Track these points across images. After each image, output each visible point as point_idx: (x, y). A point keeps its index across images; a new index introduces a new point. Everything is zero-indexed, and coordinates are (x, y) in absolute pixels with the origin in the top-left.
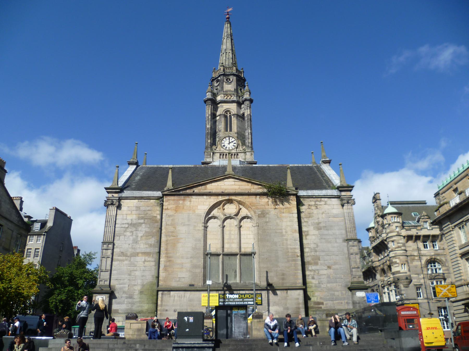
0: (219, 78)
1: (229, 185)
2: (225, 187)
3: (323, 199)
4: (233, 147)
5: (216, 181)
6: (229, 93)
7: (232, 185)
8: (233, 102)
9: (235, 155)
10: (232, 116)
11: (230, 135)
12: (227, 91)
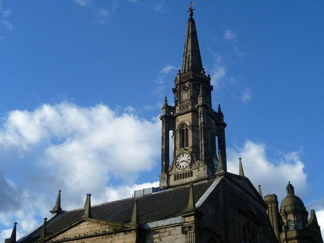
3: (167, 229)
5: (74, 226)
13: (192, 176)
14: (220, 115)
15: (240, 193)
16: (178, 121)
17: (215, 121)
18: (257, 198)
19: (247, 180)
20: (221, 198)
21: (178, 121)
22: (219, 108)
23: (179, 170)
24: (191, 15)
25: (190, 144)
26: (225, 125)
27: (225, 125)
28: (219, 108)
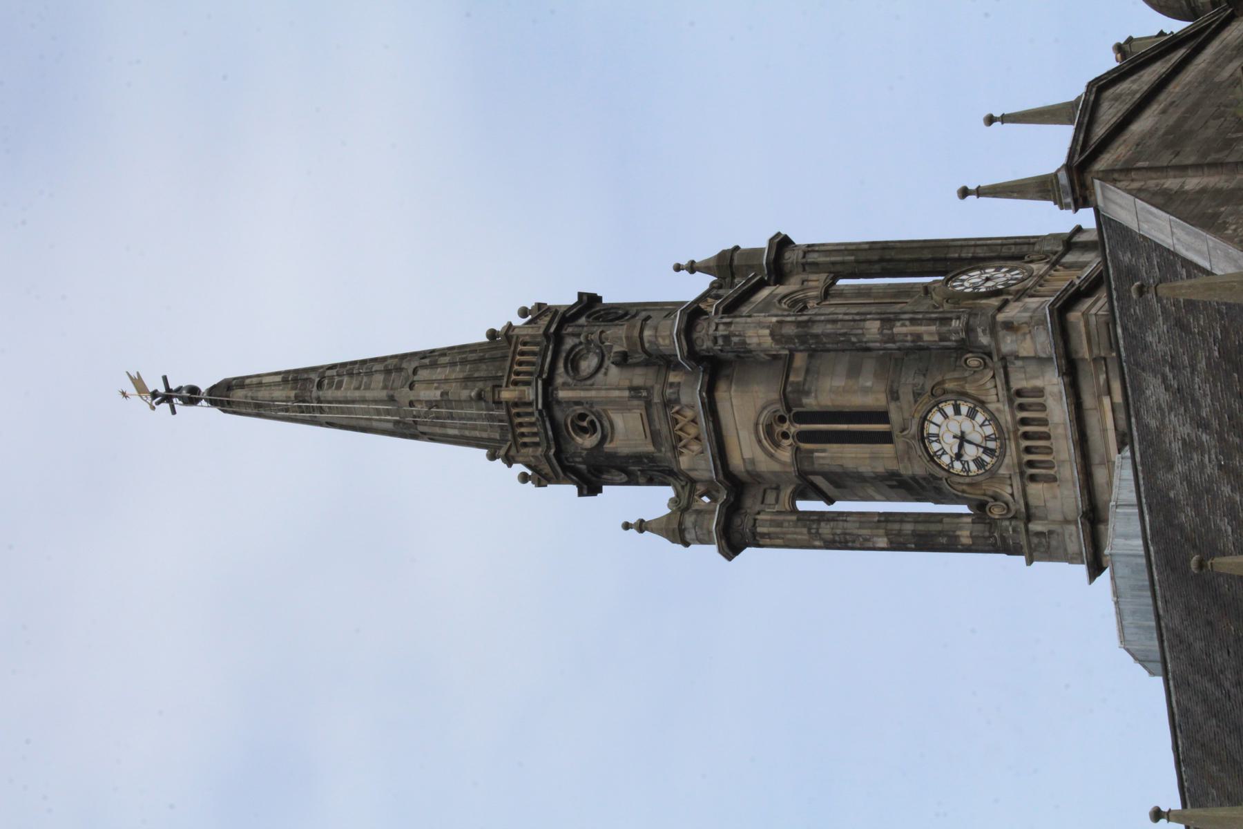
0: (583, 467)
4: (980, 418)
8: (711, 409)
9: (1022, 407)
10: (795, 410)
11: (914, 429)
12: (655, 437)
13: (1040, 392)
14: (727, 265)
15: (1164, 112)
16: (753, 461)
17: (761, 285)
18: (1181, 53)
19: (1100, 86)
20: (1193, 183)
21: (753, 461)
22: (692, 268)
23: (1007, 460)
24: (192, 396)
25: (874, 399)
26: (782, 243)
27: (782, 243)
28: (692, 268)
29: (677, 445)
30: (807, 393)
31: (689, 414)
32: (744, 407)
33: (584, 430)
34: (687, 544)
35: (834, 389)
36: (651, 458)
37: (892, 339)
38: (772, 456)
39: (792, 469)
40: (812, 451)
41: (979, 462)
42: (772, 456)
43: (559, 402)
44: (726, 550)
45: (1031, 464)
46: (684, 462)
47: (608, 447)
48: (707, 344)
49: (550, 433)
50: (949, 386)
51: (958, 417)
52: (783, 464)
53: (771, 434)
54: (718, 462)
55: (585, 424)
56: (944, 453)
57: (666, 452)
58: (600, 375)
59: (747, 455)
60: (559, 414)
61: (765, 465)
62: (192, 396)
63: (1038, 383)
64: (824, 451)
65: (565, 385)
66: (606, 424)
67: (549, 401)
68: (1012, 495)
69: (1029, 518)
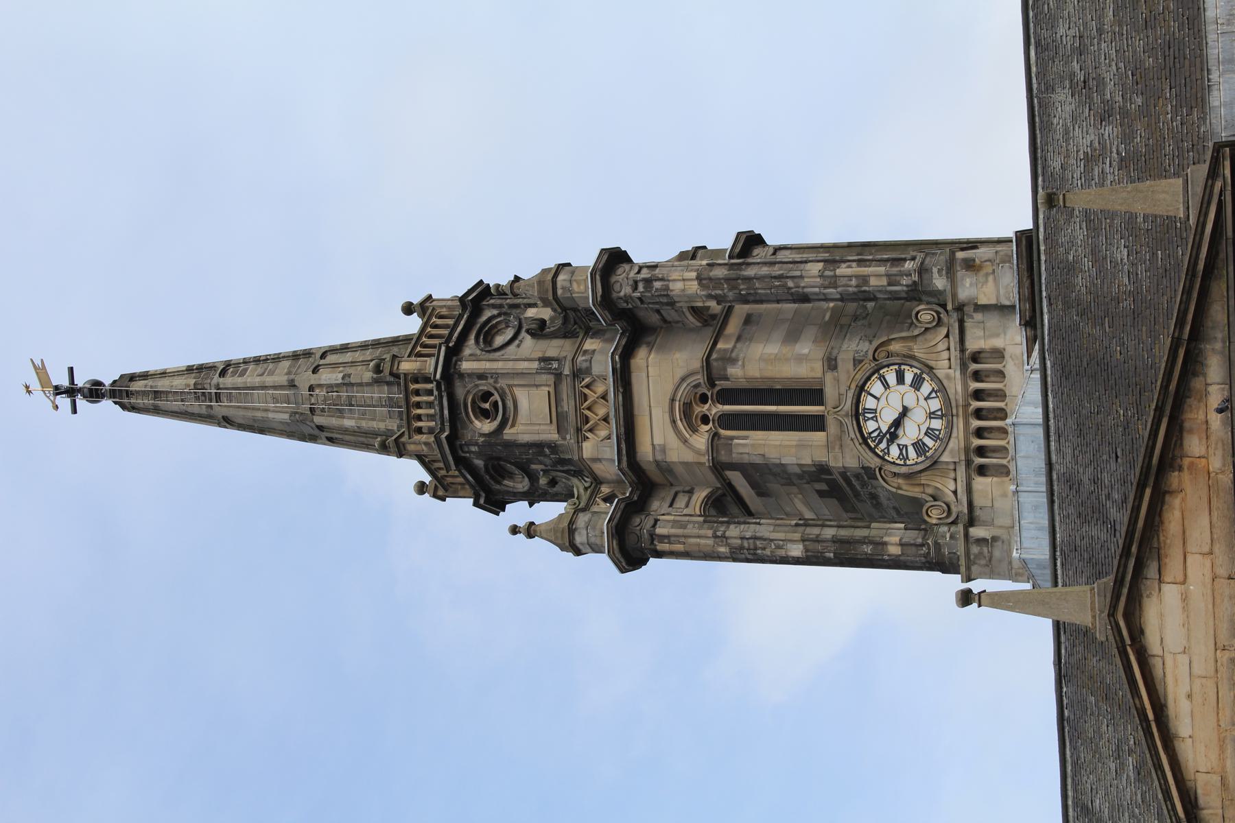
0: (479, 463)
1: (1187, 624)
2: (1203, 650)
4: (926, 388)
5: (1160, 708)
6: (568, 405)
7: (1185, 598)
8: (623, 377)
9: (977, 376)
10: (721, 384)
11: (848, 405)
12: (560, 421)
13: (999, 354)
16: (663, 449)
21: (663, 449)
24: (95, 392)
27: (750, 242)
29: (583, 427)
30: (733, 361)
31: (600, 389)
32: (662, 373)
33: (485, 414)
34: (578, 552)
35: (766, 358)
36: (553, 447)
37: (833, 282)
38: (685, 441)
39: (704, 459)
40: (732, 438)
41: (919, 446)
42: (685, 441)
43: (462, 376)
44: (618, 555)
45: (981, 451)
46: (588, 449)
47: (509, 434)
48: (626, 290)
49: (446, 412)
50: (895, 347)
51: (901, 387)
52: (698, 452)
53: (687, 413)
54: (623, 446)
55: (487, 406)
56: (875, 419)
57: (570, 439)
58: (512, 347)
59: (658, 441)
60: (460, 392)
61: (677, 453)
62: (95, 392)
63: (998, 343)
64: (745, 438)
65: (473, 357)
66: (510, 404)
67: (450, 374)
68: (955, 492)
69: (971, 522)
